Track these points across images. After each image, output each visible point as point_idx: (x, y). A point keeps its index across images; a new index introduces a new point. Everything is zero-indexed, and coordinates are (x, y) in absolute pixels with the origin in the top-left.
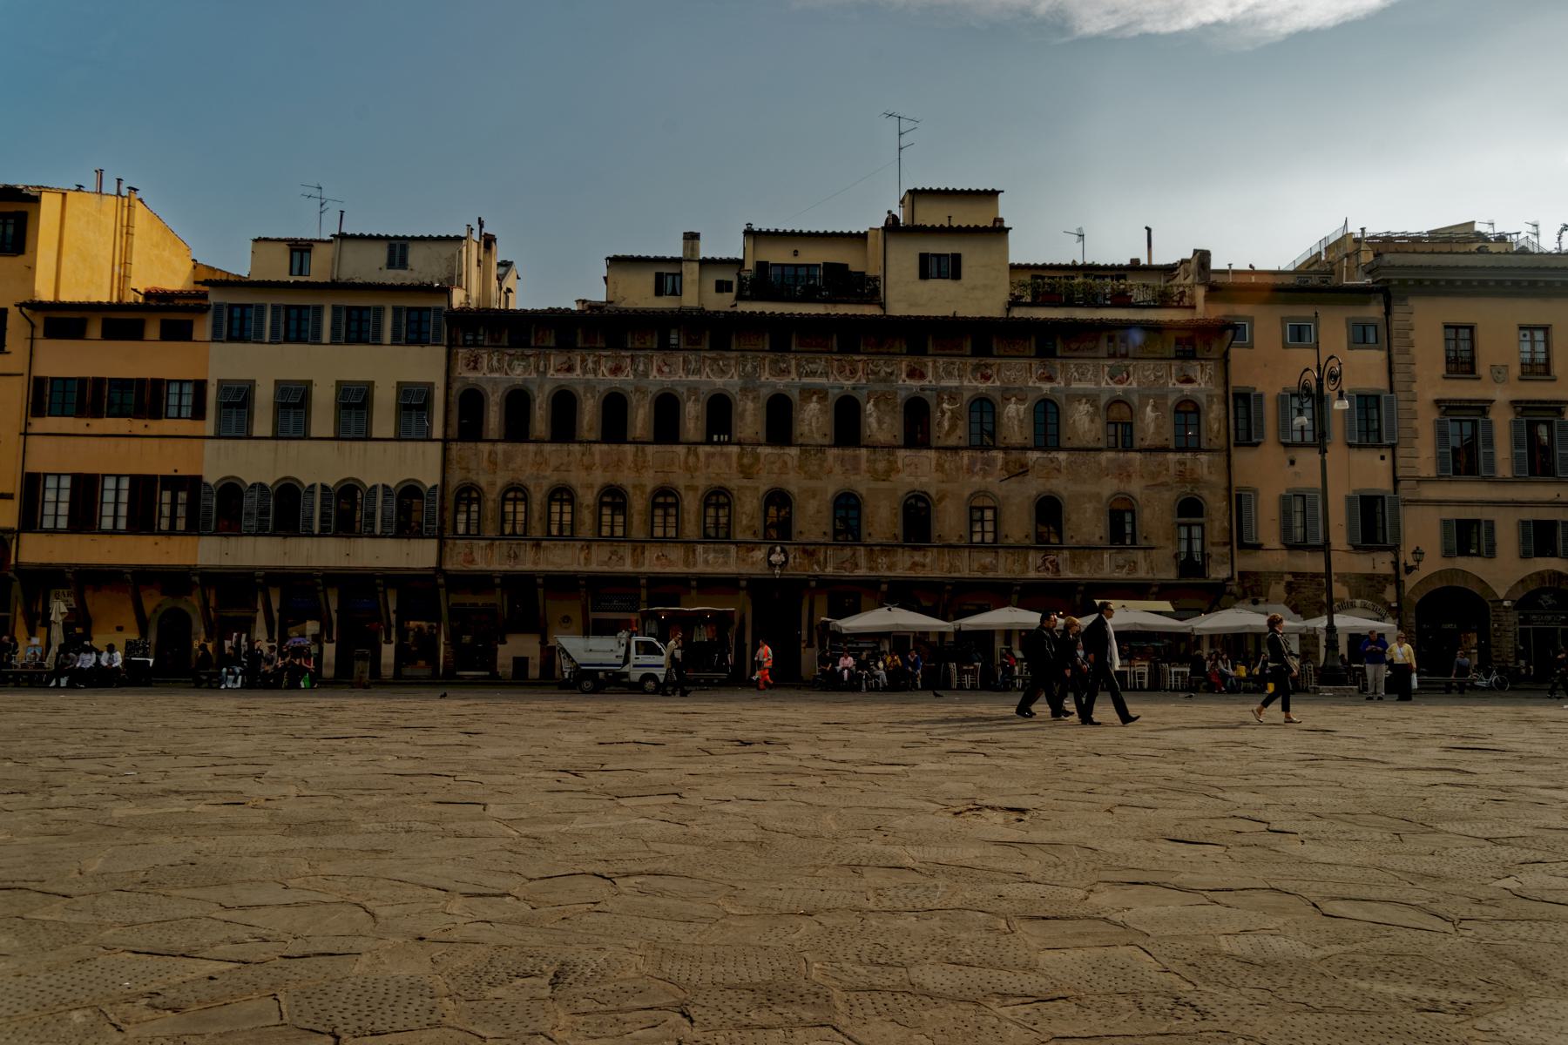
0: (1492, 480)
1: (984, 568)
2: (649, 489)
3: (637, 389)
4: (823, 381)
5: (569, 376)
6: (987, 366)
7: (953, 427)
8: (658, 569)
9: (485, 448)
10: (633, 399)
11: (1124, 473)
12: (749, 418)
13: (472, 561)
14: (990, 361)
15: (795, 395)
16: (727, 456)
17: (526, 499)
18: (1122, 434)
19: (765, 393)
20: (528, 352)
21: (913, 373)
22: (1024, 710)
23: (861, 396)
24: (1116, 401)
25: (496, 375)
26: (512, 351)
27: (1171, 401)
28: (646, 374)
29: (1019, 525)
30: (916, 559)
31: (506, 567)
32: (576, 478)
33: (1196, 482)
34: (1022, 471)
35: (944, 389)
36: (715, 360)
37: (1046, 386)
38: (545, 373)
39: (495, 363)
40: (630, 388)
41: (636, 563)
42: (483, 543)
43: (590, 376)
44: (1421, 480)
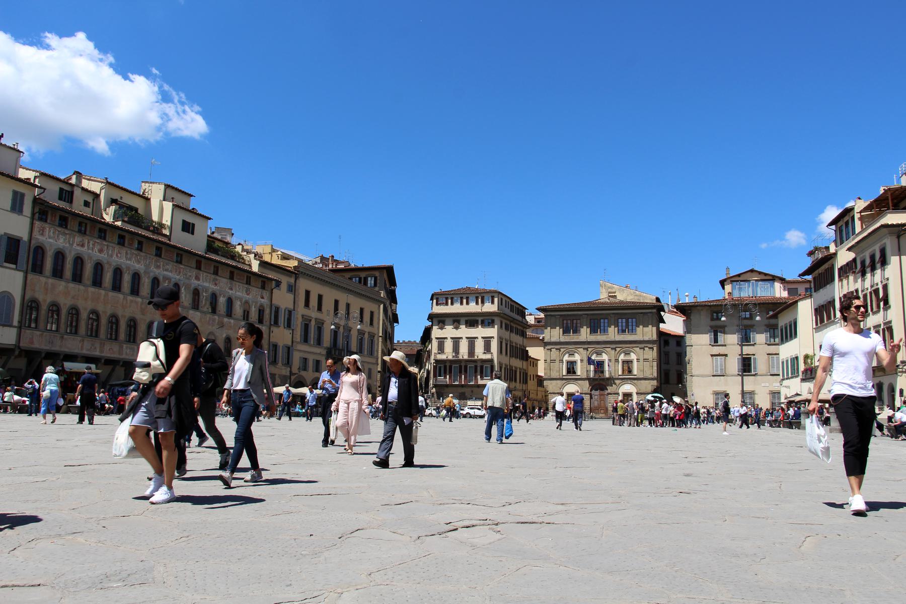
0: (311, 346)
2: (108, 314)
3: (108, 263)
4: (170, 274)
5: (82, 249)
8: (109, 355)
9: (43, 279)
10: (106, 267)
12: (146, 284)
13: (32, 343)
15: (161, 279)
16: (136, 303)
17: (38, 309)
19: (152, 275)
20: (67, 232)
21: (197, 278)
22: (81, 420)
23: (181, 284)
24: (247, 302)
25: (51, 240)
26: (60, 229)
28: (112, 256)
31: (47, 348)
32: (80, 304)
34: (222, 325)
36: (137, 255)
38: (72, 244)
39: (51, 234)
40: (105, 262)
41: (102, 351)
42: (38, 333)
43: (90, 251)
44: (298, 343)
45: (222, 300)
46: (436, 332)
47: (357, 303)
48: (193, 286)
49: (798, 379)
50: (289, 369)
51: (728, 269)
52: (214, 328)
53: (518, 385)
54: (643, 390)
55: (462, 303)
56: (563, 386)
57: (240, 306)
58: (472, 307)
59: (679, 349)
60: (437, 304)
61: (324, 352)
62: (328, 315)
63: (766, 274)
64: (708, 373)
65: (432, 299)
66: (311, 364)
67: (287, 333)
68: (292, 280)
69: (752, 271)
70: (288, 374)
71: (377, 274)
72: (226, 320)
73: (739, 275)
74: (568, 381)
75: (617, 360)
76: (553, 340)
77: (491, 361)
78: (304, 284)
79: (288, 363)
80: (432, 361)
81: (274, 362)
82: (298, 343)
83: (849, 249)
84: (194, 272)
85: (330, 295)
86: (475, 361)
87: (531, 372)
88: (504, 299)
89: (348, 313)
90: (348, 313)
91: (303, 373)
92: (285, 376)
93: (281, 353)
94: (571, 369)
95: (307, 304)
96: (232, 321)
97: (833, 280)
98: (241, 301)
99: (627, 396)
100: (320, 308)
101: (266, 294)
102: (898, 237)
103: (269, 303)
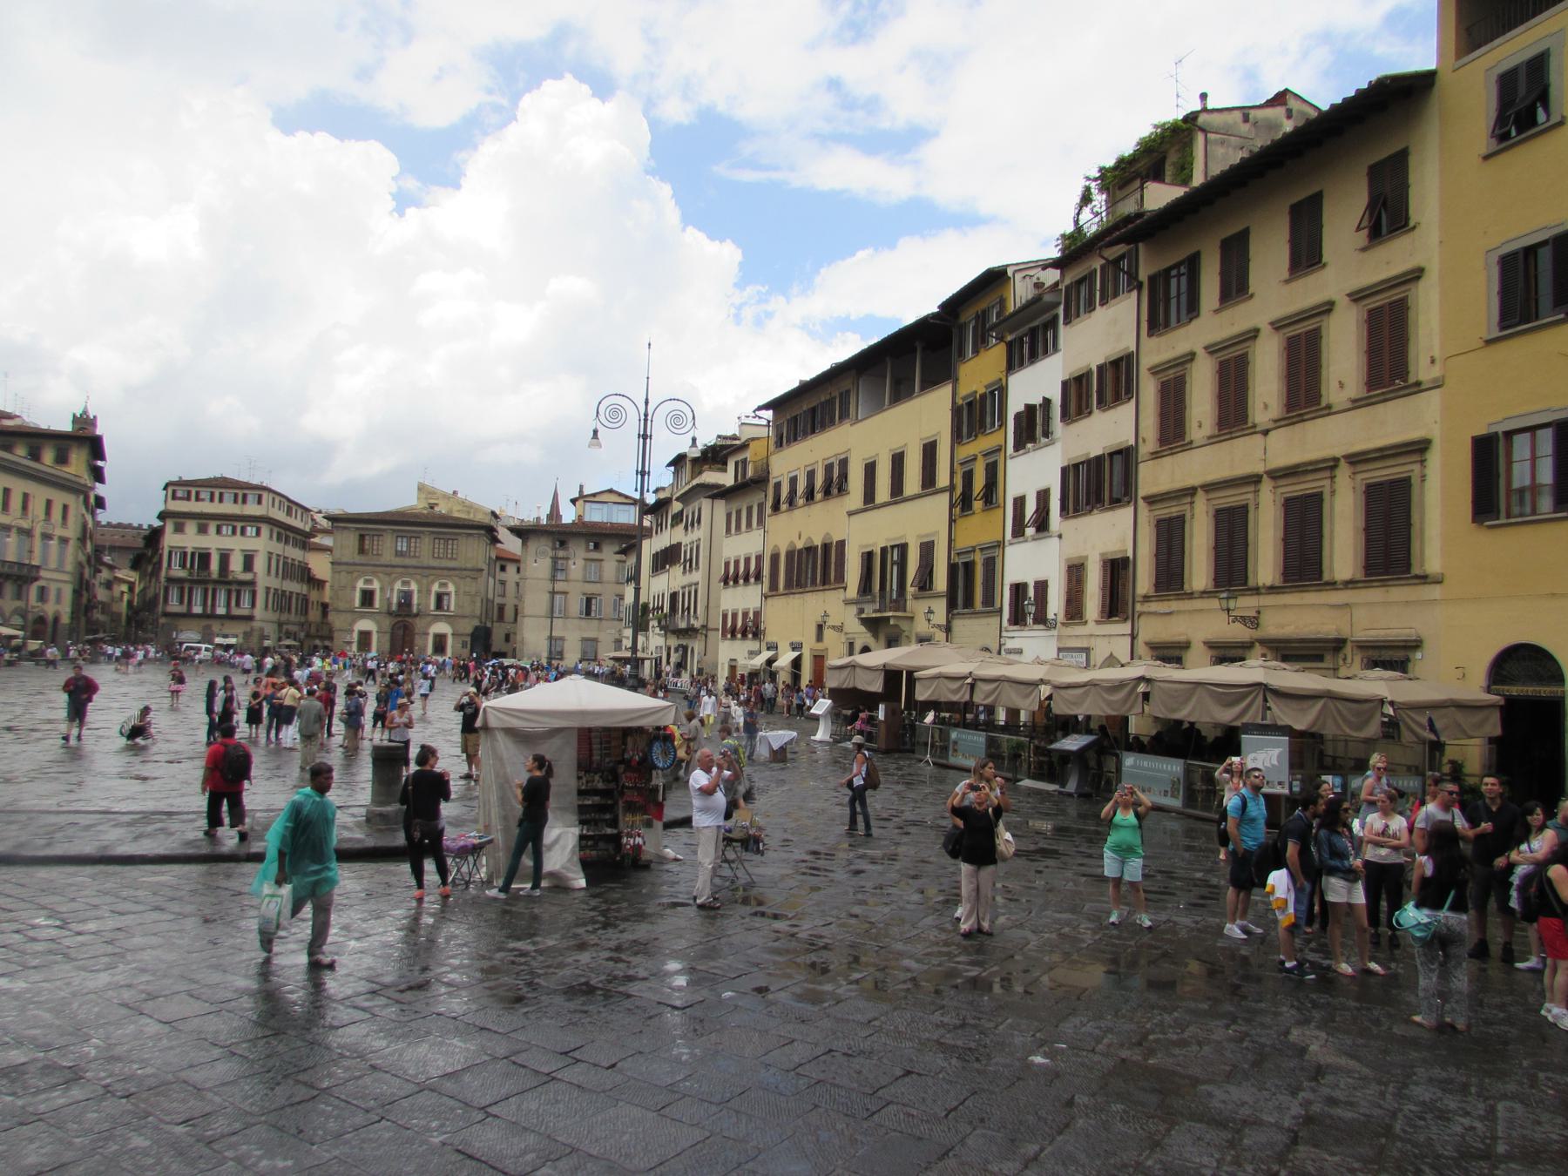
46: (170, 539)
53: (293, 617)
54: (461, 630)
55: (212, 500)
58: (228, 507)
60: (174, 497)
65: (165, 488)
69: (611, 491)
73: (594, 495)
74: (363, 616)
75: (429, 591)
77: (252, 583)
80: (163, 580)
86: (229, 583)
87: (314, 596)
88: (277, 499)
89: (25, 507)
90: (25, 507)
94: (368, 597)
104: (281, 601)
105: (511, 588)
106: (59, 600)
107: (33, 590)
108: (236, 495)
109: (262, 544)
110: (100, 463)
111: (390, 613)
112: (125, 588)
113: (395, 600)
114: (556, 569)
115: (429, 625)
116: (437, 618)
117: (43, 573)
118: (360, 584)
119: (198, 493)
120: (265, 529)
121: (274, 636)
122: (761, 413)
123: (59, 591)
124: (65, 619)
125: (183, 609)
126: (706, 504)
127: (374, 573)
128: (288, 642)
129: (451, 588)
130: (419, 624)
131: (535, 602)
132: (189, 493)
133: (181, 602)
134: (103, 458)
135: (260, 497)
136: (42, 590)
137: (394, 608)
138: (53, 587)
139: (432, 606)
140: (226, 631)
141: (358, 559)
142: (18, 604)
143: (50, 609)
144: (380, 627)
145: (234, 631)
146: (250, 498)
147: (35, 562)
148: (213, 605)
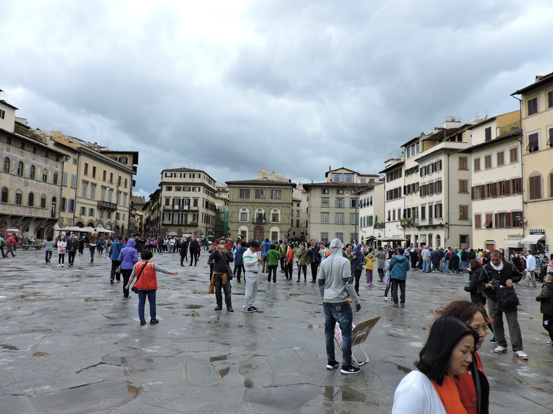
1: (18, 212)
6: (23, 152)
7: (15, 168)
11: (45, 189)
14: (24, 151)
18: (45, 178)
21: (8, 150)
27: (54, 171)
29: (25, 200)
30: (4, 207)
33: (55, 193)
34: (27, 184)
35: (14, 157)
37: (34, 161)
44: (79, 197)
45: (27, 168)
46: (165, 193)
47: (117, 174)
48: (5, 156)
49: (373, 227)
50: (73, 214)
51: (330, 167)
52: (21, 187)
54: (283, 230)
56: (239, 227)
57: (41, 172)
58: (187, 180)
59: (298, 208)
60: (166, 176)
61: (96, 204)
62: (99, 180)
63: (350, 171)
64: (319, 222)
66: (87, 212)
67: (73, 192)
68: (76, 157)
69: (343, 168)
70: (73, 217)
71: (128, 156)
72: (30, 181)
73: (336, 170)
74: (242, 224)
76: (234, 200)
77: (197, 211)
78: (84, 160)
79: (72, 209)
81: (63, 208)
82: (79, 197)
83: (416, 160)
84: (6, 146)
85: (101, 168)
88: (206, 176)
91: (82, 217)
92: (70, 219)
93: (68, 204)
95: (86, 172)
96: (35, 182)
97: (401, 176)
98: (41, 168)
99: (275, 234)
100: (94, 175)
101: (59, 165)
102: (448, 156)
103: (61, 171)
104: (207, 219)
105: (295, 213)
106: (123, 219)
107: (114, 215)
108: (190, 174)
109: (201, 195)
110: (135, 165)
111: (254, 223)
112: (139, 217)
113: (255, 218)
114: (325, 202)
115: (270, 228)
116: (273, 225)
117: (118, 207)
118: (241, 211)
119: (175, 174)
120: (202, 188)
121: (205, 234)
122: (516, 96)
123: (124, 215)
124: (126, 227)
125: (170, 222)
126: (443, 158)
127: (246, 206)
128: (210, 236)
129: (279, 212)
130: (266, 227)
131: (315, 217)
132: (172, 174)
133: (169, 220)
134: (137, 163)
135: (200, 175)
136: (118, 214)
137: (255, 221)
138: (122, 214)
139: (271, 220)
140: (187, 231)
141: (240, 200)
142: (109, 220)
143: (120, 223)
144: (249, 229)
145: (190, 232)
146: (196, 176)
147: (114, 201)
148: (182, 220)
